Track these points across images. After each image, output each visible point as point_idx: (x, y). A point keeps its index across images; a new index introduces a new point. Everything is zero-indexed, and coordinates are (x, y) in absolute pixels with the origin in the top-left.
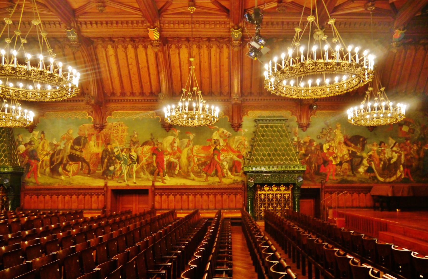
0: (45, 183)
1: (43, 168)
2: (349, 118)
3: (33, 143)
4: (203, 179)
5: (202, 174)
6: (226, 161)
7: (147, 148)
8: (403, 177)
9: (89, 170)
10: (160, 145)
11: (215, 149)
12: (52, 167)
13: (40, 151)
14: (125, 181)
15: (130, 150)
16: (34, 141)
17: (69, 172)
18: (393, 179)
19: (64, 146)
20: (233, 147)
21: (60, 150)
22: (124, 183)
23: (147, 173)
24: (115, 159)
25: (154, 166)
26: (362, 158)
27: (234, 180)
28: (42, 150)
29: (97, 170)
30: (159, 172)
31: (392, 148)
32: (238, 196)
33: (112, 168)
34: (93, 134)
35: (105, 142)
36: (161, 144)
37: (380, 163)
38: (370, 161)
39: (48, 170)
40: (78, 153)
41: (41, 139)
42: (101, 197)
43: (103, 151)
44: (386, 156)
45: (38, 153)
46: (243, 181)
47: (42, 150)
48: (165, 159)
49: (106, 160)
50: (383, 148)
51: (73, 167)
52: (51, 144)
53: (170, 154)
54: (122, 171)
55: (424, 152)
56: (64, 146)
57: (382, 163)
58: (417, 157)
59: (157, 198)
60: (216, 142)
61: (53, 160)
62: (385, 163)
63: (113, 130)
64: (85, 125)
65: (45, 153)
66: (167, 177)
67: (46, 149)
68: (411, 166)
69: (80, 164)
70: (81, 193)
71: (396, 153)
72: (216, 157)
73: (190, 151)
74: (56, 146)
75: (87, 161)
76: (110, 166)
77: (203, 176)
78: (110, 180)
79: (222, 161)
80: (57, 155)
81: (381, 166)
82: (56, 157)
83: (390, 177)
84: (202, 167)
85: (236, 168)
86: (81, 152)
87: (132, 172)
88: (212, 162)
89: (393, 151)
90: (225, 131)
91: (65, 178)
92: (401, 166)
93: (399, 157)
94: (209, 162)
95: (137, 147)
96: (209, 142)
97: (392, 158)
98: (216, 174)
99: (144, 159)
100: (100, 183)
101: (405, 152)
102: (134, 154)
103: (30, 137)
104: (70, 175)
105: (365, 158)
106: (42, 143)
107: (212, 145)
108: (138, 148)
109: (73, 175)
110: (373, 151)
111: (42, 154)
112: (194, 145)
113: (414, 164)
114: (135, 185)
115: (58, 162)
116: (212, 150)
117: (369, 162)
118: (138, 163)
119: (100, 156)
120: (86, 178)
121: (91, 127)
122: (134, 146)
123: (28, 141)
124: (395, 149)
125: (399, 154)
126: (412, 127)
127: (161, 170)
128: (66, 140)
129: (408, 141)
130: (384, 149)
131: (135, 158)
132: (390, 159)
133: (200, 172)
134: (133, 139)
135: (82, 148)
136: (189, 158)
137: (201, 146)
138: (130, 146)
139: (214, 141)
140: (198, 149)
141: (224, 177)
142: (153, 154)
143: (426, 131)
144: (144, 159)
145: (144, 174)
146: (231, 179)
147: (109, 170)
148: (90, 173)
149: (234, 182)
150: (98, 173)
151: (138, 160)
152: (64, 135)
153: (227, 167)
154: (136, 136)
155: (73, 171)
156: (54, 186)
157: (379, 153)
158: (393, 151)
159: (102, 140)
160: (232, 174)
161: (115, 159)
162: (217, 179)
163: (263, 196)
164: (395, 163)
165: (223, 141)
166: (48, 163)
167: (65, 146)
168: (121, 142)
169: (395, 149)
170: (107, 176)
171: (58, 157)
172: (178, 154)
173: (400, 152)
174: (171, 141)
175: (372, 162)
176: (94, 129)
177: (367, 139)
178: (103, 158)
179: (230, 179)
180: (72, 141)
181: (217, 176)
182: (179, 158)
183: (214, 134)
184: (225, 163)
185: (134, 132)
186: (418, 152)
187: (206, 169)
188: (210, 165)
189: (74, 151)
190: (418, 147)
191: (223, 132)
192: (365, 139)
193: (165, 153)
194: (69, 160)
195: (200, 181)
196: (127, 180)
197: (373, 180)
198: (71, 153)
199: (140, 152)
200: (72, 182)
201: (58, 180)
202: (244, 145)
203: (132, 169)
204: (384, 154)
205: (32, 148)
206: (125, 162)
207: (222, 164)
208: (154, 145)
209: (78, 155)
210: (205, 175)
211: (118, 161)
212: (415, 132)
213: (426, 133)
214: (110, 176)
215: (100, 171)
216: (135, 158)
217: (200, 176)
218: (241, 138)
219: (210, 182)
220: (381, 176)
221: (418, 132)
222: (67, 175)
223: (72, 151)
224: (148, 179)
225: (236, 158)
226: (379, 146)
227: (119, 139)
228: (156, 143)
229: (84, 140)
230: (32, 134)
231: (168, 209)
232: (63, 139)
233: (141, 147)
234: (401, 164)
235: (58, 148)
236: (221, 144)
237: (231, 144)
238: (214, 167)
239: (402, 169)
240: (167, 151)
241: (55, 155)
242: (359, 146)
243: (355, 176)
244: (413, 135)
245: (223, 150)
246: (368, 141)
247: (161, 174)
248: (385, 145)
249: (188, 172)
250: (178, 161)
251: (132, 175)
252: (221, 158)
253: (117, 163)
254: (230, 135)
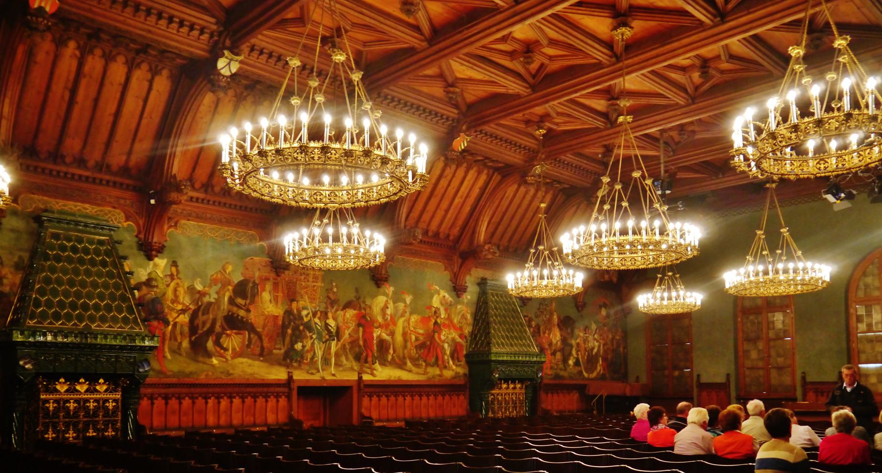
0: (179, 372)
1: (176, 340)
2: (509, 287)
3: (154, 283)
4: (421, 371)
7: (350, 313)
9: (262, 348)
10: (368, 311)
11: (436, 323)
12: (193, 338)
13: (169, 303)
14: (319, 371)
15: (325, 315)
16: (156, 280)
17: (226, 350)
18: (594, 375)
19: (216, 296)
20: (455, 321)
21: (210, 304)
22: (318, 374)
23: (351, 357)
24: (303, 330)
25: (360, 346)
27: (456, 373)
28: (173, 302)
29: (276, 349)
30: (367, 356)
32: (462, 397)
33: (299, 346)
34: (267, 279)
35: (288, 295)
36: (370, 307)
39: (185, 344)
40: (242, 313)
41: (172, 276)
42: (283, 401)
43: (285, 313)
45: (165, 306)
46: (465, 374)
47: (173, 302)
48: (375, 335)
49: (289, 331)
51: (233, 341)
52: (191, 290)
53: (380, 326)
54: (315, 353)
56: (216, 296)
59: (366, 400)
60: (436, 312)
61: (196, 323)
63: (301, 275)
64: (255, 258)
65: (180, 307)
66: (377, 365)
67: (181, 299)
69: (244, 337)
70: (249, 393)
72: (436, 335)
73: (406, 324)
74: (202, 294)
75: (259, 330)
76: (296, 342)
78: (296, 368)
79: (443, 342)
80: (203, 314)
82: (201, 318)
86: (248, 311)
87: (330, 354)
90: (447, 296)
91: (219, 361)
93: (599, 346)
95: (337, 310)
98: (436, 364)
99: (347, 332)
100: (279, 374)
102: (332, 323)
103: (149, 271)
104: (229, 358)
106: (173, 285)
108: (339, 312)
109: (233, 358)
111: (173, 309)
112: (411, 314)
114: (334, 378)
115: (205, 329)
118: (338, 340)
119: (280, 323)
120: (257, 363)
121: (264, 264)
122: (332, 307)
123: (144, 278)
124: (596, 336)
127: (370, 354)
128: (219, 285)
131: (333, 330)
132: (593, 348)
133: (418, 359)
134: (331, 296)
135: (250, 304)
136: (404, 334)
137: (419, 317)
138: (327, 308)
140: (416, 322)
141: (445, 367)
142: (359, 325)
144: (347, 332)
145: (347, 359)
147: (295, 350)
148: (263, 355)
150: (277, 354)
151: (338, 335)
152: (217, 273)
153: (448, 352)
154: (335, 290)
155: (234, 349)
156: (197, 379)
159: (283, 292)
161: (303, 330)
162: (437, 371)
163: (51, 406)
166: (186, 329)
167: (219, 298)
168: (312, 300)
169: (596, 336)
170: (291, 360)
171: (205, 317)
172: (391, 327)
174: (382, 305)
176: (268, 269)
178: (284, 327)
179: (454, 370)
180: (230, 288)
181: (438, 366)
182: (392, 334)
184: (446, 346)
185: (332, 283)
189: (235, 309)
193: (375, 325)
194: (226, 327)
195: (418, 373)
196: (323, 370)
198: (229, 312)
199: (340, 319)
200: (231, 371)
201: (205, 367)
202: (466, 319)
203: (330, 348)
205: (152, 295)
206: (320, 338)
207: (443, 347)
208: (360, 309)
209: (242, 318)
211: (308, 334)
214: (296, 361)
215: (279, 352)
216: (333, 330)
217: (418, 366)
219: (430, 375)
222: (222, 356)
223: (231, 307)
224: (352, 369)
225: (459, 340)
227: (309, 292)
228: (363, 306)
229: (253, 287)
230: (151, 263)
231: (179, 428)
232: (215, 281)
233: (342, 310)
235: (206, 299)
240: (377, 321)
241: (200, 313)
243: (565, 370)
247: (370, 359)
249: (404, 358)
250: (392, 338)
251: (330, 360)
252: (443, 337)
253: (306, 337)
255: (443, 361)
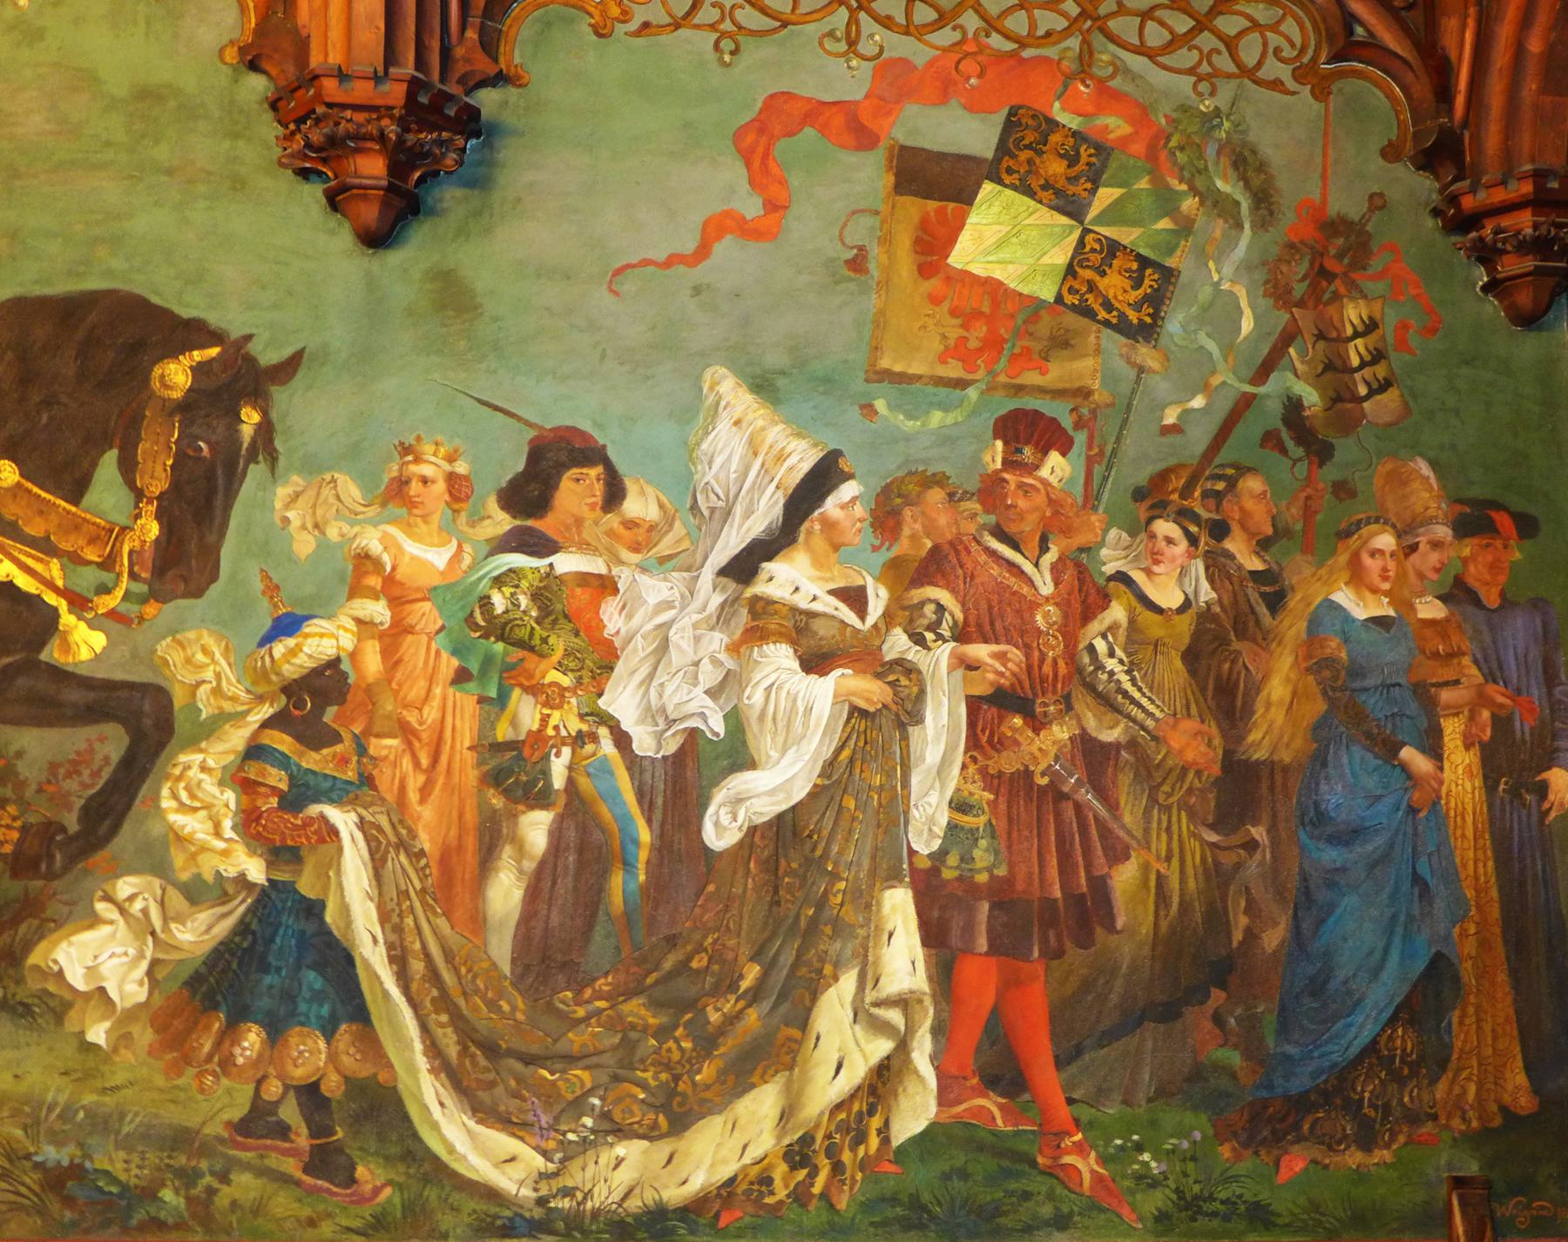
8: (915, 1112)
26: (147, 723)
31: (743, 568)
37: (492, 838)
38: (301, 792)
44: (622, 701)
50: (566, 563)
55: (1317, 665)
57: (536, 828)
58: (1193, 743)
62: (584, 846)
68: (1091, 909)
71: (815, 662)
81: (505, 893)
83: (676, 1115)
89: (764, 623)
92: (898, 906)
93: (874, 736)
97: (737, 754)
101: (980, 651)
105: (209, 730)
110: (379, 611)
113: (1124, 878)
117: (281, 819)
124: (793, 579)
125: (871, 691)
126: (1127, 236)
129: (1056, 468)
130: (605, 586)
143: (1353, 313)
157: (500, 646)
158: (764, 623)
164: (783, 836)
173: (897, 643)
175: (342, 819)
177: (289, 368)
186: (1215, 658)
190: (1218, 567)
192: (240, 379)
197: (328, 1163)
204: (600, 660)
212: (1174, 324)
213: (1355, 352)
220: (488, 1072)
221: (1222, 315)
226: (502, 522)
234: (891, 863)
239: (903, 960)
242: (107, 492)
244: (1146, 354)
246: (305, 412)
248: (614, 494)
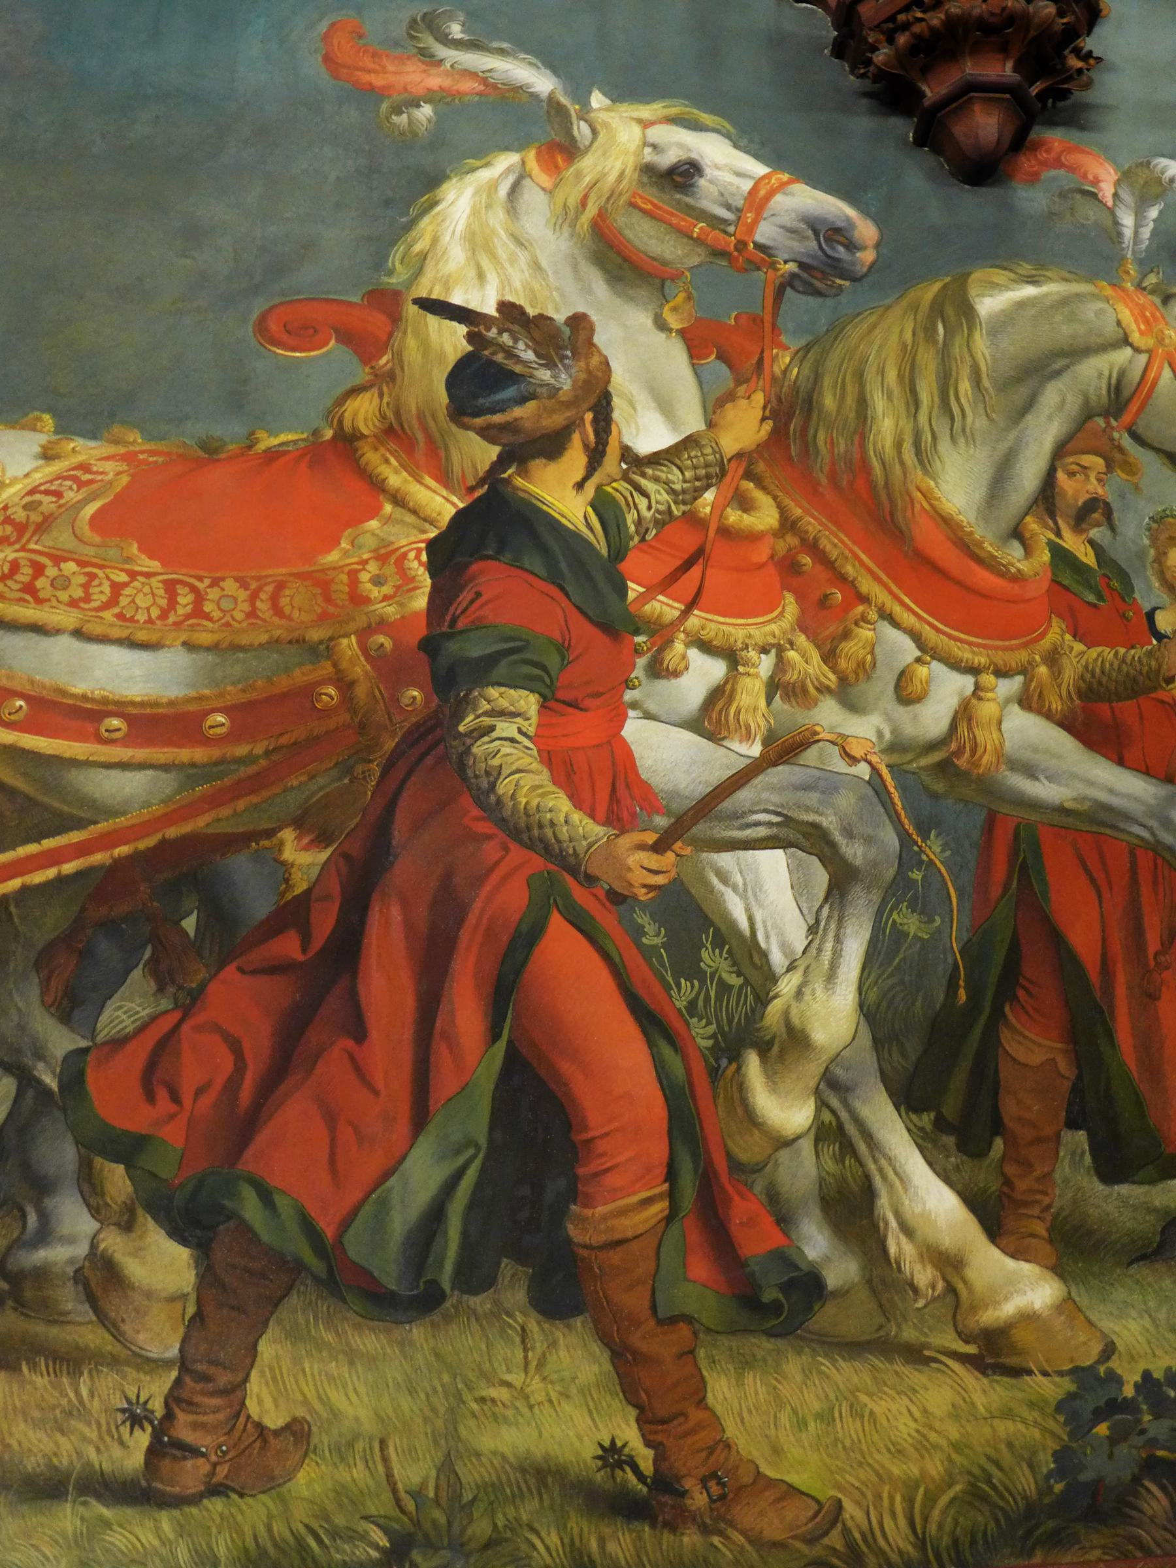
5: (75, 1229)
6: (799, 836)
11: (493, 525)
27: (1092, 1396)
72: (509, 736)
77: (101, 1280)
79: (700, 820)
84: (72, 1005)
85: (1086, 1029)
88: (410, 867)
90: (728, 166)
94: (304, 859)
96: (329, 361)
98: (522, 1226)
107: (394, 433)
116: (412, 541)
139: (452, 340)
141: (779, 1306)
146: (995, 1352)
149: (1107, 1460)
153: (832, 1013)
160: (994, 1215)
165: (674, 358)
181: (563, 1288)
183: (460, 201)
184: (766, 893)
187: (202, 1064)
188: (346, 950)
191: (683, 176)
207: (691, 919)
210: (163, 1265)
218: (1112, 309)
236: (647, 432)
237: (887, 424)
238: (465, 1012)
245: (697, 557)
252: (666, 753)
254: (833, 233)
255: (707, 1171)
